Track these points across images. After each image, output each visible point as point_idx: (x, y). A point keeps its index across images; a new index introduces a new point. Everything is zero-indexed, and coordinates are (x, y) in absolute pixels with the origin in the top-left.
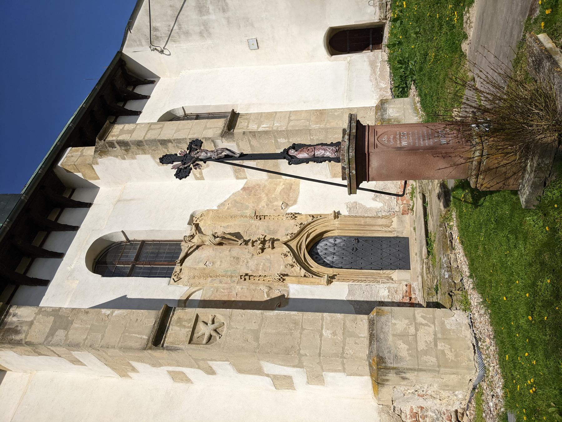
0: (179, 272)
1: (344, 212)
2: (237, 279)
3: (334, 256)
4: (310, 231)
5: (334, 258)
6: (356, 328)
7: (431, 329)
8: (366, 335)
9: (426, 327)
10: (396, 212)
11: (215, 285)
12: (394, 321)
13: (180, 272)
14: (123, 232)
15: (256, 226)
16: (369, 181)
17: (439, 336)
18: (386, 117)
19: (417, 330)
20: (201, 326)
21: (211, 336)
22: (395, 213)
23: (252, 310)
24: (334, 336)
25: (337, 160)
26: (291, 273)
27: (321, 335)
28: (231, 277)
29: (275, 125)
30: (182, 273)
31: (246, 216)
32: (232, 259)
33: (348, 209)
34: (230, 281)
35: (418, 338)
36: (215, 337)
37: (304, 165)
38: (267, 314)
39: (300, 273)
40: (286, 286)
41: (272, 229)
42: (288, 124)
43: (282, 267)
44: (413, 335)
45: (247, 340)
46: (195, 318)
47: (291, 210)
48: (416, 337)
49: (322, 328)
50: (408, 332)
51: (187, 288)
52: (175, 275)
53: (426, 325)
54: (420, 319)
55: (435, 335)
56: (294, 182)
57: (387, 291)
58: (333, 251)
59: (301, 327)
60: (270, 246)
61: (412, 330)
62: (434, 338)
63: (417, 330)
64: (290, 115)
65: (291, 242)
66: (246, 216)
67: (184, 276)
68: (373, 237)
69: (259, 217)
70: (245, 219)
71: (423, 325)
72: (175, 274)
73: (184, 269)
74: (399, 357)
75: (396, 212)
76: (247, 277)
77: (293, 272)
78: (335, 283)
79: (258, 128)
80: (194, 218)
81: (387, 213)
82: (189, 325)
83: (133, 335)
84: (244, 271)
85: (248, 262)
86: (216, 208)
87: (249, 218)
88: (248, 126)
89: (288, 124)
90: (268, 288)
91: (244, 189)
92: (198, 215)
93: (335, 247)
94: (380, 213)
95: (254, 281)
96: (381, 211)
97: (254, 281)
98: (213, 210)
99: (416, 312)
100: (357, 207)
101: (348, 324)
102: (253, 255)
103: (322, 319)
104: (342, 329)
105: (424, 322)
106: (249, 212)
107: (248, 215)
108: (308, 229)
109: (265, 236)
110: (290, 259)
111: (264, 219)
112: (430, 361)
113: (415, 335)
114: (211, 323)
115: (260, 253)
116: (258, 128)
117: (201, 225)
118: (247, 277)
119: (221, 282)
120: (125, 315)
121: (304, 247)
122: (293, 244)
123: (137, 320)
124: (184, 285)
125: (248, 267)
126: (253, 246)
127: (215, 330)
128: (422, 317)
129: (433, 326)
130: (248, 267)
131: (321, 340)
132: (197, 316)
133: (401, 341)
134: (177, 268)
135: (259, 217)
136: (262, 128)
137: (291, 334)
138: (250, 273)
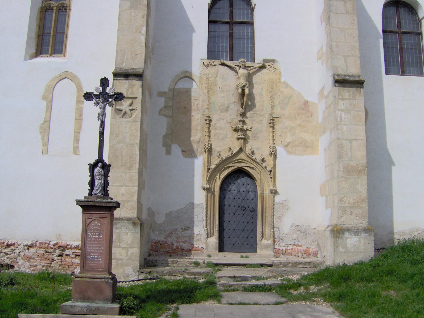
0: (213, 65)
1: (277, 199)
2: (207, 113)
3: (236, 192)
4: (257, 169)
5: (235, 191)
6: (127, 209)
7: (123, 257)
8: (122, 216)
9: (125, 254)
10: (279, 243)
11: (201, 97)
12: (129, 234)
13: (213, 66)
14: (255, 4)
15: (261, 120)
17: (120, 262)
18: (347, 234)
19: (124, 248)
20: (129, 102)
21: (122, 111)
22: (278, 243)
23: (139, 136)
24: (121, 194)
25: (90, 194)
26: (213, 157)
27: (121, 186)
28: (209, 109)
29: (344, 127)
30: (212, 68)
31: (272, 109)
32: (226, 105)
33: (281, 202)
34: (204, 108)
35: (118, 249)
36: (120, 114)
37: (89, 174)
38: (137, 147)
39: (214, 164)
40: (201, 154)
41: (258, 135)
42: (346, 140)
43: (218, 149)
44: (120, 245)
45: (118, 136)
46: (134, 96)
47: (280, 150)
48: (119, 247)
49: (127, 186)
50: (122, 243)
51: (198, 75)
52: (210, 62)
53: (127, 255)
54: (131, 251)
55: (120, 259)
56: (315, 149)
57: (198, 233)
58: (241, 190)
59: (127, 171)
60: (239, 136)
61: (123, 245)
62: (118, 259)
63: (124, 248)
64: (359, 140)
65: (244, 154)
66: (272, 109)
67: (211, 70)
68: (257, 223)
69: (272, 122)
70: (269, 109)
71: (127, 253)
72: (211, 62)
73: (216, 68)
75: (279, 243)
76: (207, 122)
77: (214, 158)
78: (204, 193)
79: (341, 110)
80: (271, 63)
81: (277, 235)
82: (129, 94)
83: (126, 56)
84: (214, 118)
85: (223, 120)
86: (282, 80)
87: (271, 112)
88: (343, 99)
89: (346, 140)
90: (198, 140)
91: (306, 103)
92: (276, 65)
93: (245, 192)
94: (277, 230)
95: (205, 127)
96: (280, 231)
97: (205, 127)
98: (280, 78)
99: (136, 249)
100: (284, 210)
101: (130, 204)
102: (230, 123)
103: (133, 186)
104: (126, 200)
105: (129, 254)
106: (277, 111)
107: (274, 111)
108: (258, 167)
109: (250, 131)
110: (225, 155)
111: (270, 127)
113: (120, 247)
114: (131, 109)
115: (232, 128)
116: (341, 110)
117: (264, 71)
118: (207, 122)
119: (203, 101)
120: (141, 44)
121: (240, 165)
122: (242, 156)
123: (137, 55)
124: (201, 72)
125: (218, 120)
126: (240, 121)
127: (125, 113)
128: (133, 253)
129: (126, 259)
130: (218, 120)
131: (118, 186)
132: (136, 98)
133: (116, 238)
134: (217, 62)
135: (272, 122)
136: (341, 114)
137: (122, 166)
138: (212, 123)
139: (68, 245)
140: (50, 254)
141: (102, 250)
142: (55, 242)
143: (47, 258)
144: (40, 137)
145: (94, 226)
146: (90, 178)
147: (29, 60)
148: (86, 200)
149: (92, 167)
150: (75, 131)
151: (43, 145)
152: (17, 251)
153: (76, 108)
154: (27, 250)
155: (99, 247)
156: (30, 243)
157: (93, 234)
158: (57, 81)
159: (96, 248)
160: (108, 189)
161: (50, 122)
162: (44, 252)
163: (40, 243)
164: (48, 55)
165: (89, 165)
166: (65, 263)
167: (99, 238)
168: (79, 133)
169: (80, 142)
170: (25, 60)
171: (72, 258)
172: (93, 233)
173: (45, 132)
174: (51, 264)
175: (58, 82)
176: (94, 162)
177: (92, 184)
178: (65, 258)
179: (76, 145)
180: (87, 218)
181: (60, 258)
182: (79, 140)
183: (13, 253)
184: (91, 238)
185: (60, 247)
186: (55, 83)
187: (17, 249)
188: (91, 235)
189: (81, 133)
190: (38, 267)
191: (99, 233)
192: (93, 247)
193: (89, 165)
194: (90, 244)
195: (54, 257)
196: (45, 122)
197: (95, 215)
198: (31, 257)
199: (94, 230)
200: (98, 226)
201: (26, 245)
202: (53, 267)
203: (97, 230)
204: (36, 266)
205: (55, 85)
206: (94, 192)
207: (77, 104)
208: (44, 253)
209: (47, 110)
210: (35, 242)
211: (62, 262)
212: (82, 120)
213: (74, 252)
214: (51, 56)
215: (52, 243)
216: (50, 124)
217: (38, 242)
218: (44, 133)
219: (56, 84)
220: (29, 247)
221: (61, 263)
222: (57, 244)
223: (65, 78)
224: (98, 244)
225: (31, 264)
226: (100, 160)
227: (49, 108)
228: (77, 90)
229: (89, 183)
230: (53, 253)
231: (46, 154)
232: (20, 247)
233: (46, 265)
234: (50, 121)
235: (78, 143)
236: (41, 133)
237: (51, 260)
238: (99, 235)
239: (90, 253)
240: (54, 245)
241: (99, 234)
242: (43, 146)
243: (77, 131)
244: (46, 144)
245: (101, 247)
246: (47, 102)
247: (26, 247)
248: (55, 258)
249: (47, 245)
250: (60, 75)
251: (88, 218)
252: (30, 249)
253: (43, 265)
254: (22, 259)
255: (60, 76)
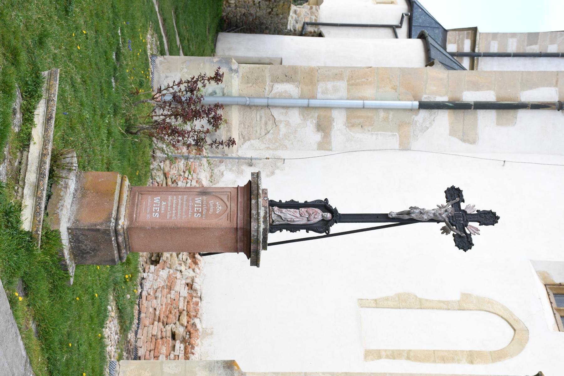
16: (237, 188)
25: (272, 204)
37: (309, 200)
74: (207, 370)
112: (171, 368)
139: (193, 348)
140: (177, 319)
141: (171, 217)
142: (199, 326)
143: (171, 313)
144: (391, 294)
145: (215, 205)
146: (302, 201)
147: (536, 272)
148: (261, 191)
149: (323, 203)
150: (410, 351)
151: (376, 300)
152: (183, 268)
153: (456, 351)
154: (184, 282)
155: (176, 213)
156: (196, 286)
157: (200, 204)
158: (504, 317)
159: (174, 209)
160: (284, 231)
161: (421, 308)
162: (180, 307)
163: (197, 304)
164: (555, 305)
165: (326, 199)
166: (159, 344)
167: (193, 213)
168: (408, 358)
169: (391, 361)
170: (533, 262)
171: (168, 354)
172: (202, 204)
173: (400, 301)
174: (159, 321)
175: (502, 317)
176: (331, 206)
177: (293, 205)
178: (169, 344)
179: (383, 354)
180: (229, 194)
181: (169, 334)
182: (394, 358)
183: (180, 262)
184: (193, 200)
185: (190, 335)
186: (500, 314)
187: (187, 268)
188: (198, 200)
189: (409, 361)
190: (155, 301)
191: (201, 213)
192: (177, 204)
193: (326, 199)
194: (182, 200)
195: (170, 326)
196: (420, 300)
197: (234, 205)
198: (172, 288)
199: (208, 204)
200: (215, 210)
201: (193, 280)
202: (153, 324)
203: (208, 210)
204: (156, 298)
205: (495, 313)
206: (276, 208)
207: (465, 353)
208: (178, 308)
209: (444, 302)
210: (199, 295)
211: (162, 338)
212: (434, 361)
213: (180, 357)
214: (554, 310)
215: (197, 321)
216: (418, 308)
217: (200, 301)
218: (399, 300)
219: (498, 315)
220: (190, 286)
221: (159, 336)
222: (197, 330)
223: (515, 330)
224: (182, 212)
225: (160, 289)
226: (338, 218)
227: (446, 306)
228: (495, 352)
229: (292, 201)
230: (178, 323)
231: (361, 304)
232: (191, 271)
233: (157, 313)
234: (424, 308)
235: (387, 357)
236: (399, 296)
237: (165, 320)
238: (198, 212)
239: (166, 200)
240: (194, 325)
241: (199, 213)
242: (373, 300)
243: (412, 354)
244: (377, 304)
245: (176, 216)
246: (459, 301)
247: (189, 281)
248: (169, 328)
249: (193, 314)
250: (518, 321)
251: (229, 196)
252: (187, 288)
253: (157, 309)
254: (169, 276)
255: (515, 320)
